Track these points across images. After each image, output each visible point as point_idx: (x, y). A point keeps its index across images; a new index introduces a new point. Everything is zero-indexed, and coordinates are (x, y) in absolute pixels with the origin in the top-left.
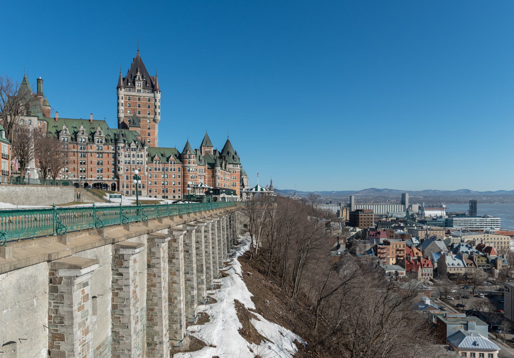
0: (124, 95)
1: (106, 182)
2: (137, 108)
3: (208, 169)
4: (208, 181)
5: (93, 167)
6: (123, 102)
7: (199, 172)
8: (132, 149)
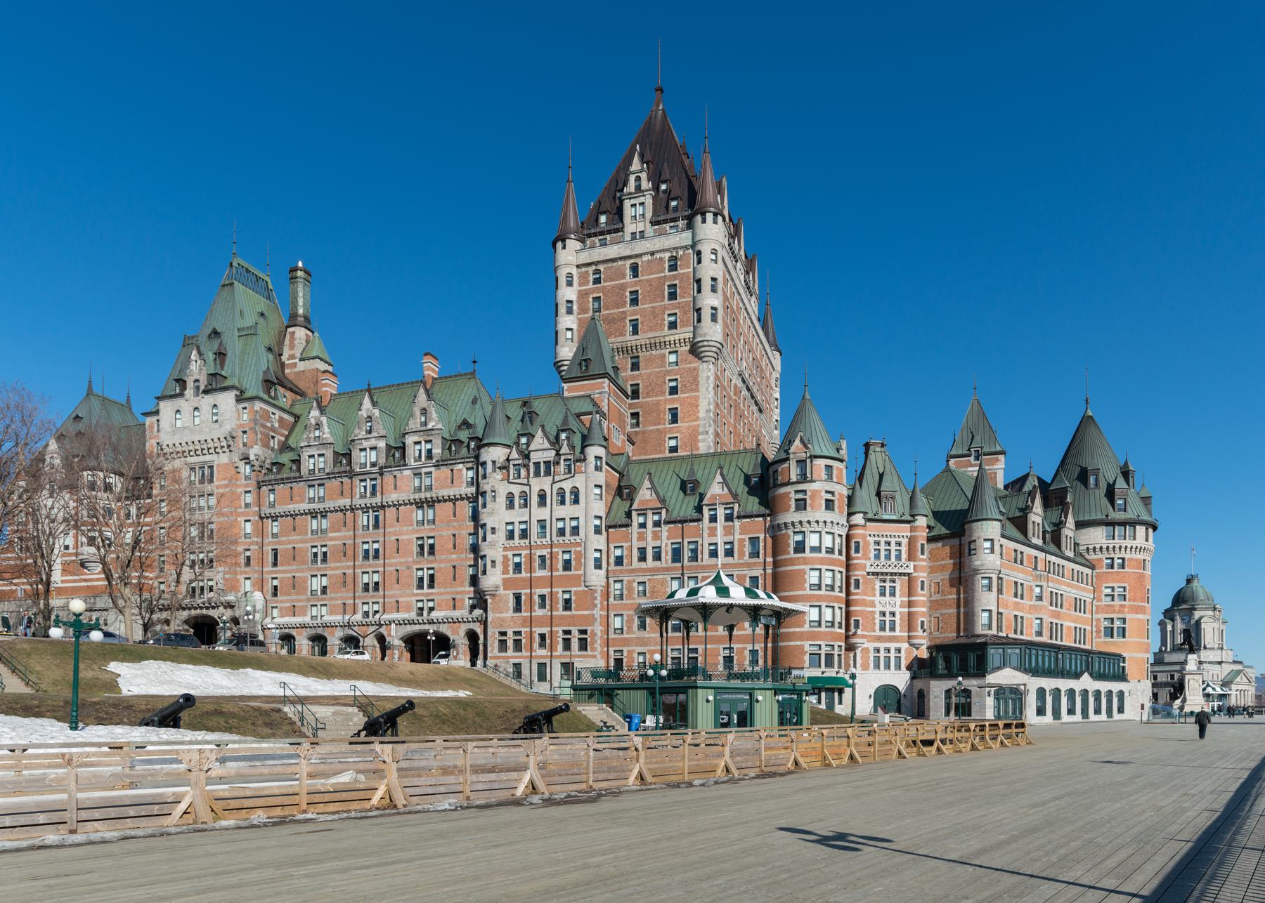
0: (578, 266)
1: (445, 629)
2: (628, 308)
3: (930, 540)
4: (934, 605)
5: (404, 568)
6: (574, 297)
7: (877, 557)
8: (537, 464)
